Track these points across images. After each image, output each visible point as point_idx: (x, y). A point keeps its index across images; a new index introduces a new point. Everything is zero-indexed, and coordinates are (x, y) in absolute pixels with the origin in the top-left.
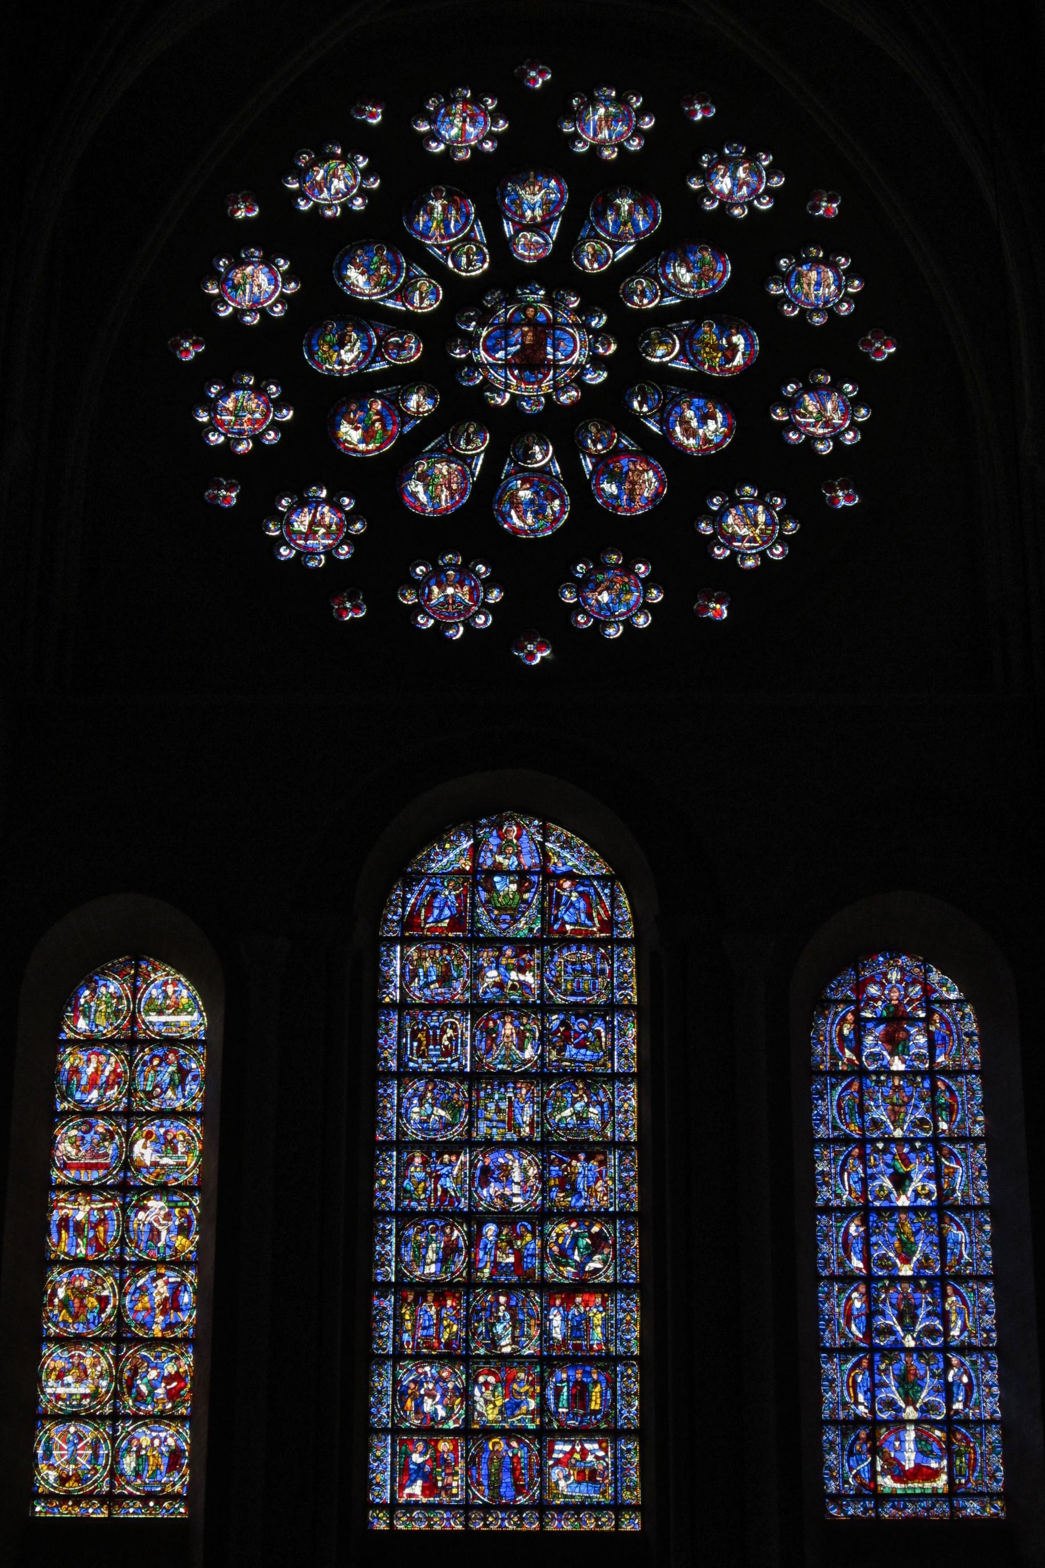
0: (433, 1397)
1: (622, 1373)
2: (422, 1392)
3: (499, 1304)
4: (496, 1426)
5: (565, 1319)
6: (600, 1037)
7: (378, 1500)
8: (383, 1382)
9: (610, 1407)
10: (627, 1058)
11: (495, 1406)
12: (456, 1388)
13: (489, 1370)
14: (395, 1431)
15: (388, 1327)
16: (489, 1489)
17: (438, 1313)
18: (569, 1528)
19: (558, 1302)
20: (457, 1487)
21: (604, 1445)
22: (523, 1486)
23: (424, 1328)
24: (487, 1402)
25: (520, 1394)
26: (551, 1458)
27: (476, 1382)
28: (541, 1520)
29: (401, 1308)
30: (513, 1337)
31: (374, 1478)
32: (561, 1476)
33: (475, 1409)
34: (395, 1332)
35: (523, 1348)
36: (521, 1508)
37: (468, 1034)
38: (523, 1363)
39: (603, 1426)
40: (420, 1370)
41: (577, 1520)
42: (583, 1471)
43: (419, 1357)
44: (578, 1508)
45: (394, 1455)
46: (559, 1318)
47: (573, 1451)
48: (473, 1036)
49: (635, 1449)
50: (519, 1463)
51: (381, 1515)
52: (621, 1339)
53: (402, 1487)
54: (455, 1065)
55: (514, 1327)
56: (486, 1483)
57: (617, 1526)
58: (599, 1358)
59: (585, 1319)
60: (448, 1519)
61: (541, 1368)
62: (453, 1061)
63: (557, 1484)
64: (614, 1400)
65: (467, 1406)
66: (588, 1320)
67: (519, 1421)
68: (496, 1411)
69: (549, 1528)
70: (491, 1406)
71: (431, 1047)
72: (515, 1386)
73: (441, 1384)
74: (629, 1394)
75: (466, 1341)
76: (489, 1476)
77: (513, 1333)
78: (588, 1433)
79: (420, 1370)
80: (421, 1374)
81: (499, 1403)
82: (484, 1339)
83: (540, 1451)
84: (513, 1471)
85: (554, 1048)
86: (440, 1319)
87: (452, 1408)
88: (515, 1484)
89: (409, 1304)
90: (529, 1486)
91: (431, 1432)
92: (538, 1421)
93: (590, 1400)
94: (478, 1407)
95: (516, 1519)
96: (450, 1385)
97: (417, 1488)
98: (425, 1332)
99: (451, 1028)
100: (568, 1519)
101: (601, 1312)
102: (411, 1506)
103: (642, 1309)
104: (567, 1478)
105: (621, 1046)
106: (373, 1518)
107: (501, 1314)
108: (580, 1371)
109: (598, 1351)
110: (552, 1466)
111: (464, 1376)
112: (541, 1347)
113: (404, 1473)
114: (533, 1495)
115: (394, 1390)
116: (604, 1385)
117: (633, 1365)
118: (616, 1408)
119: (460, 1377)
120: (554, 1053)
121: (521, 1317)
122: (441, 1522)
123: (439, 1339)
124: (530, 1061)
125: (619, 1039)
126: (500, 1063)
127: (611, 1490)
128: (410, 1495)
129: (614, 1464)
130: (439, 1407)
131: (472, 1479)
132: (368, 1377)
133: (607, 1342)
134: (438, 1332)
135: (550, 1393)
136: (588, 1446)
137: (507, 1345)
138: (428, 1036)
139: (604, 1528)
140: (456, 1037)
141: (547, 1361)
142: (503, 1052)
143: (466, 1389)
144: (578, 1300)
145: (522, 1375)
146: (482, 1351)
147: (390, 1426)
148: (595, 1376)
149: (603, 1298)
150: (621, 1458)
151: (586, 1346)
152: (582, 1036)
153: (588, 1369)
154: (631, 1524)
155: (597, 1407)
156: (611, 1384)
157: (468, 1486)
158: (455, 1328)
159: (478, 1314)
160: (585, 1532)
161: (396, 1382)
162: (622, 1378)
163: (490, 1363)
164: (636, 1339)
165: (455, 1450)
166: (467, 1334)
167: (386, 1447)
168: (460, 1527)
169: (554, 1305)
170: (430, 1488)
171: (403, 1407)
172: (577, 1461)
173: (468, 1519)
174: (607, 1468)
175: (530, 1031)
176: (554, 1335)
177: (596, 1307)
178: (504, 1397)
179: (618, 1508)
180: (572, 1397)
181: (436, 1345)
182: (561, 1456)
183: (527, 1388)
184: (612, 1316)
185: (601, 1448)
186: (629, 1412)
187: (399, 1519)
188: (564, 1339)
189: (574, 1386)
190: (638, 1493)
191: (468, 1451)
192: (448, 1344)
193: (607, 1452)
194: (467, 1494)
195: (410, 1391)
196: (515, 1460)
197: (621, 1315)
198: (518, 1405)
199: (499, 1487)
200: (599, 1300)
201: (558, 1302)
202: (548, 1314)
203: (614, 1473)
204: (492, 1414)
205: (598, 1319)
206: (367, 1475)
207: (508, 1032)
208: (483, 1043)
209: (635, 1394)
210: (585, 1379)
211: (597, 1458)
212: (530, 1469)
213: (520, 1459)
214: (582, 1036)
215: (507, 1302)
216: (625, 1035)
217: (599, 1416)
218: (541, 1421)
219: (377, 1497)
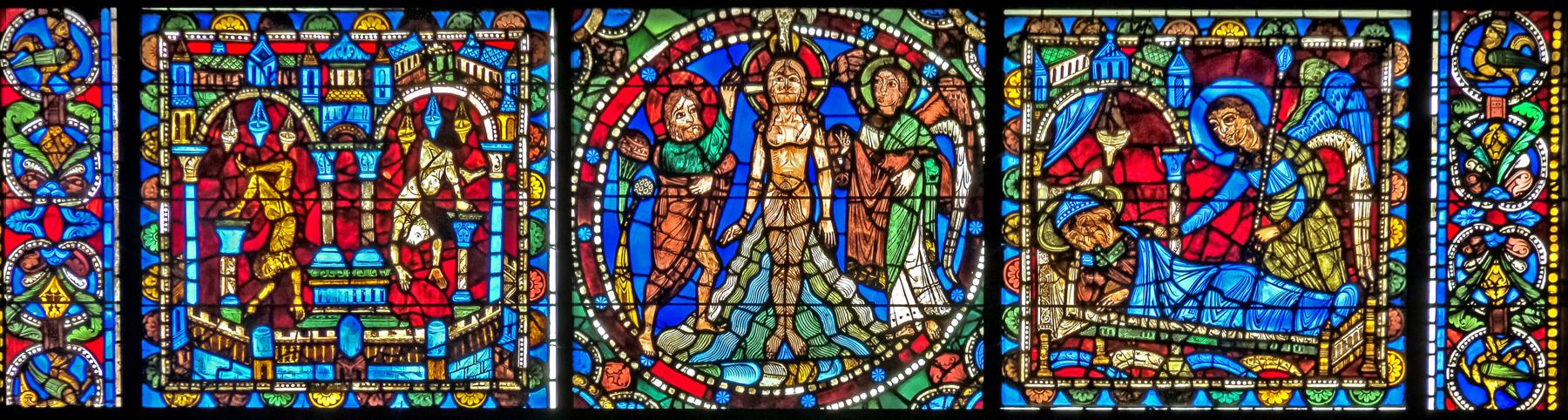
6: (1339, 198)
10: (1496, 319)
37: (541, 185)
48: (574, 196)
54: (474, 365)
62: (457, 348)
71: (328, 257)
85: (1061, 262)
99: (446, 139)
105: (1469, 250)
120: (1063, 290)
124: (918, 342)
125: (1454, 204)
126: (740, 355)
138: (302, 197)
140: (478, 194)
142: (758, 292)
152: (1234, 187)
175: (918, 153)
207: (791, 164)
208: (639, 234)
214: (1234, 187)
216: (1489, 177)
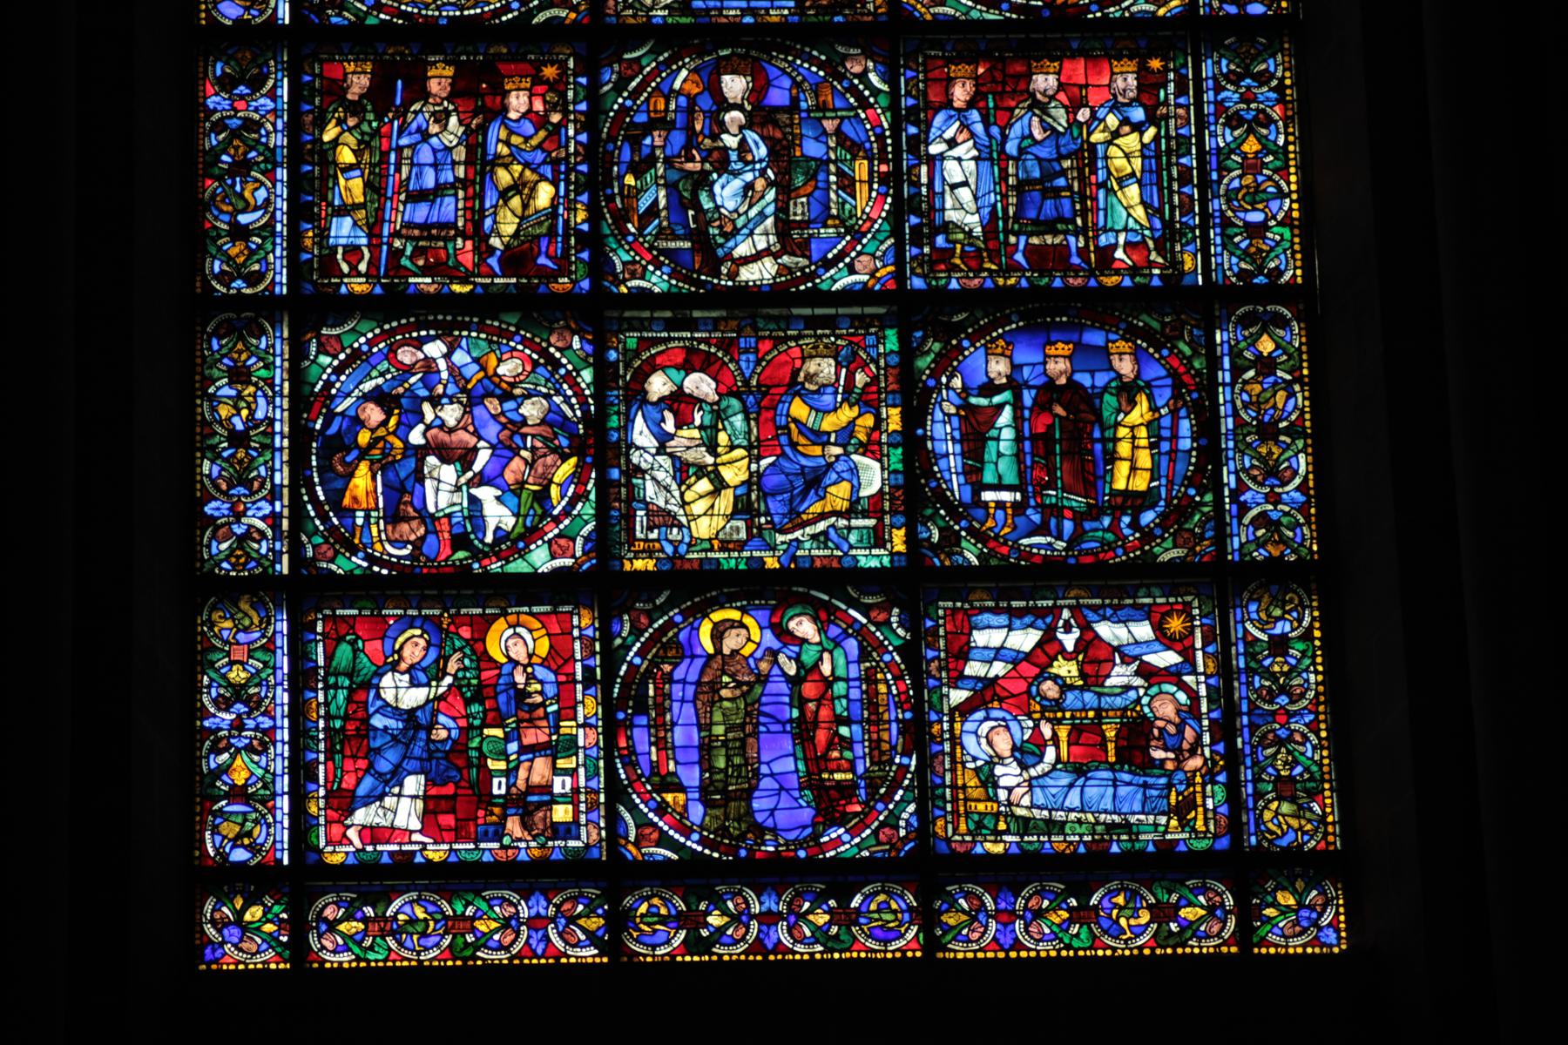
0: (465, 458)
1: (1235, 354)
2: (416, 437)
3: (724, 105)
4: (729, 561)
5: (993, 155)
7: (240, 855)
8: (249, 398)
9: (1190, 481)
11: (719, 485)
12: (553, 420)
13: (690, 351)
14: (304, 592)
15: (267, 197)
16: (707, 803)
17: (474, 141)
18: (1047, 950)
19: (960, 93)
20: (573, 797)
21: (1175, 625)
22: (847, 790)
23: (419, 196)
24: (683, 471)
25: (820, 438)
26: (957, 679)
27: (636, 395)
28: (927, 918)
29: (322, 125)
30: (784, 227)
31: (225, 769)
32: (1003, 744)
33: (633, 498)
34: (298, 211)
35: (829, 264)
36: (840, 879)
38: (830, 323)
39: (1169, 553)
40: (406, 356)
41: (1076, 916)
42: (1096, 726)
43: (399, 309)
44: (1083, 870)
45: (301, 678)
46: (965, 150)
47: (1048, 648)
49: (1307, 636)
50: (826, 697)
51: (254, 913)
52: (1226, 223)
53: (343, 803)
55: (786, 192)
56: (691, 777)
57: (1245, 934)
58: (1140, 298)
59: (1075, 155)
60: (536, 923)
61: (903, 339)
63: (989, 781)
64: (1210, 452)
65: (603, 485)
66: (1088, 156)
67: (821, 539)
68: (725, 502)
69: (960, 951)
70: (704, 485)
72: (799, 409)
73: (493, 405)
74: (1268, 432)
75: (593, 240)
76: (706, 749)
77: (782, 209)
78: (1116, 582)
79: (406, 356)
80: (408, 370)
81: (734, 474)
82: (661, 233)
83: (910, 652)
84: (803, 731)
86: (481, 163)
87: (542, 497)
88: (812, 782)
89: (355, 108)
90: (872, 787)
91: (456, 586)
92: (898, 540)
93: (1112, 458)
94: (651, 489)
95: (821, 919)
96: (532, 410)
97: (404, 809)
98: (420, 213)
100: (1039, 914)
101: (1138, 128)
102: (378, 878)
103: (1305, 116)
104: (1026, 754)
106: (220, 925)
107: (731, 141)
108: (1063, 349)
109: (1134, 271)
110: (965, 709)
111: (587, 375)
112: (899, 261)
113: (356, 745)
114: (892, 822)
115: (300, 435)
116: (1164, 396)
117: (1284, 323)
118: (1218, 486)
119: (571, 379)
121: (813, 149)
122: (502, 930)
123: (479, 235)
127: (1214, 798)
128: (372, 834)
129: (1222, 694)
130: (486, 494)
131: (630, 764)
132: (189, 384)
133: (1168, 237)
134: (476, 217)
135: (942, 433)
136: (1107, 631)
137: (757, 257)
139: (1194, 948)
141: (928, 312)
143: (596, 423)
144: (1044, 82)
145: (825, 368)
146: (657, 281)
147: (284, 567)
148: (1126, 367)
149: (1142, 72)
150: (1250, 672)
151: (1083, 253)
153: (1095, 338)
154: (1302, 926)
155: (1141, 483)
156: (1196, 396)
157: (617, 793)
158: (544, 195)
159: (636, 143)
160: (1115, 962)
161: (304, 400)
162: (1237, 371)
163: (692, 325)
164: (1287, 222)
165: (558, 659)
166: (594, 216)
167: (270, 647)
168: (589, 953)
169: (948, 104)
170: (459, 795)
171: (335, 497)
172: (1065, 687)
173: (619, 921)
174: (1193, 710)
176: (952, 216)
177: (1115, 107)
178: (755, 450)
179: (1246, 868)
180: (1034, 447)
181: (468, 259)
182: (999, 668)
183: (846, 414)
184: (1183, 141)
185: (1165, 639)
186: (1275, 499)
187: (332, 926)
188: (989, 227)
189: (1041, 406)
190: (1327, 805)
191: (611, 658)
192: (517, 257)
193: (1188, 654)
194: (613, 819)
195: (364, 438)
196: (809, 689)
197: (1222, 137)
198: (815, 481)
199: (748, 795)
200: (1127, 82)
201: (960, 93)
202: (917, 143)
203: (1224, 730)
204: (708, 519)
205: (1125, 154)
206: (194, 761)
209: (1294, 431)
210: (1084, 379)
211: (1149, 673)
212: (875, 721)
213: (828, 683)
215: (757, 93)
217: (1148, 517)
218: (911, 539)
219: (236, 842)
